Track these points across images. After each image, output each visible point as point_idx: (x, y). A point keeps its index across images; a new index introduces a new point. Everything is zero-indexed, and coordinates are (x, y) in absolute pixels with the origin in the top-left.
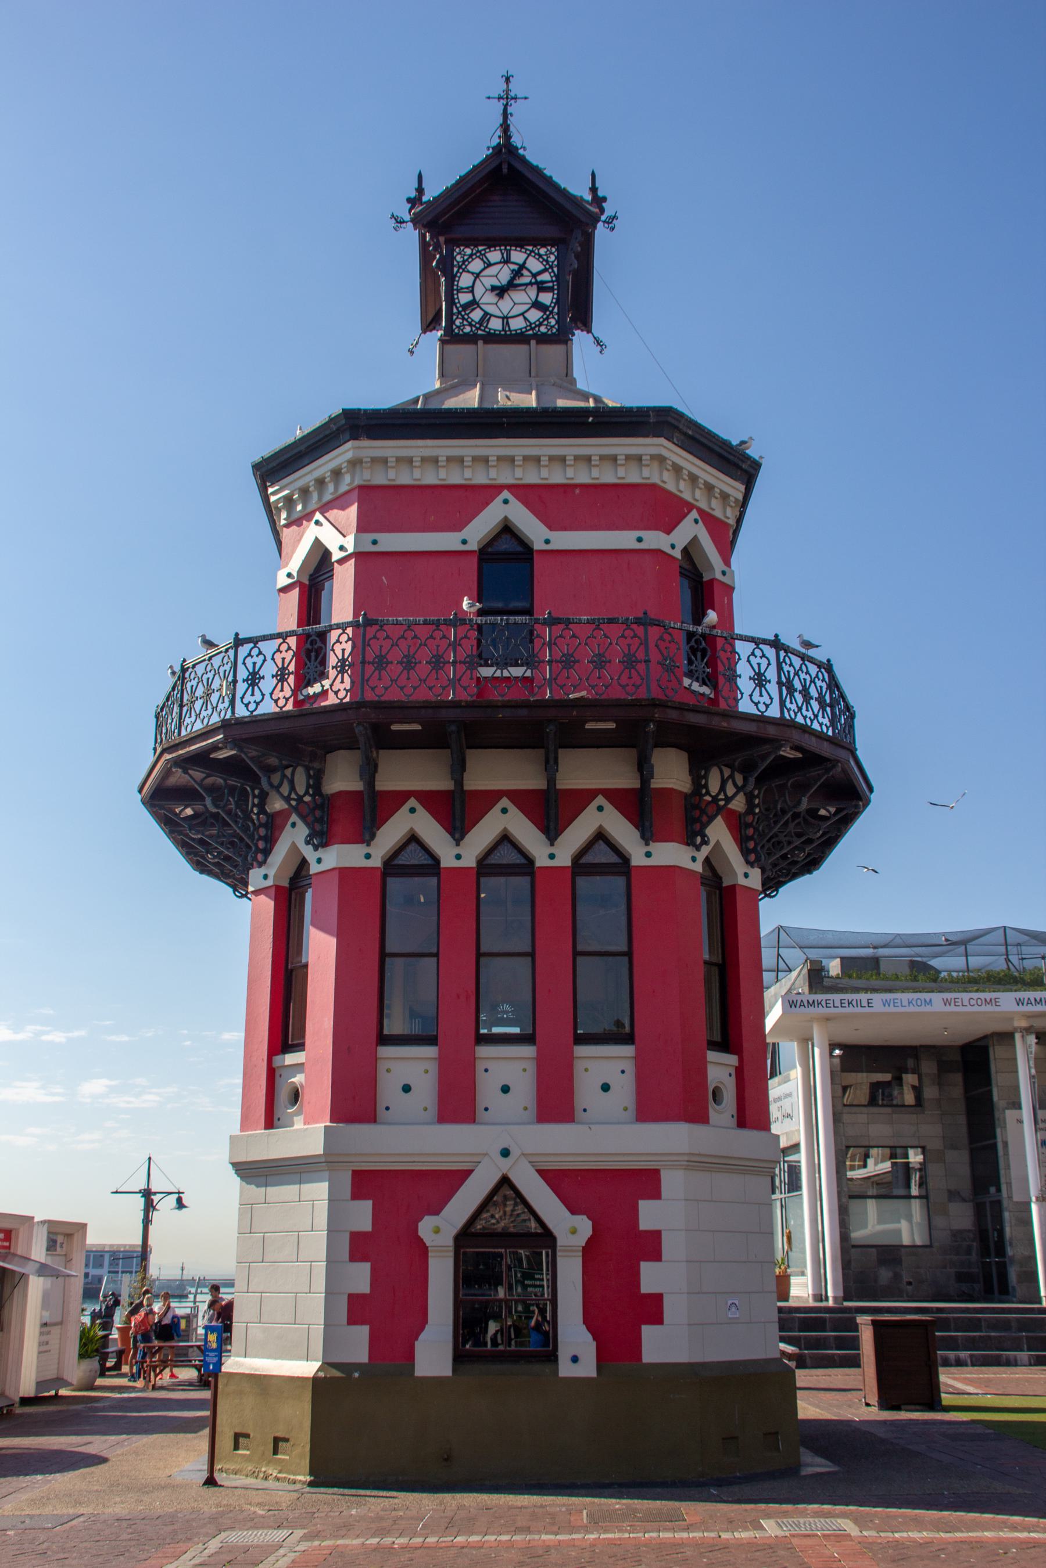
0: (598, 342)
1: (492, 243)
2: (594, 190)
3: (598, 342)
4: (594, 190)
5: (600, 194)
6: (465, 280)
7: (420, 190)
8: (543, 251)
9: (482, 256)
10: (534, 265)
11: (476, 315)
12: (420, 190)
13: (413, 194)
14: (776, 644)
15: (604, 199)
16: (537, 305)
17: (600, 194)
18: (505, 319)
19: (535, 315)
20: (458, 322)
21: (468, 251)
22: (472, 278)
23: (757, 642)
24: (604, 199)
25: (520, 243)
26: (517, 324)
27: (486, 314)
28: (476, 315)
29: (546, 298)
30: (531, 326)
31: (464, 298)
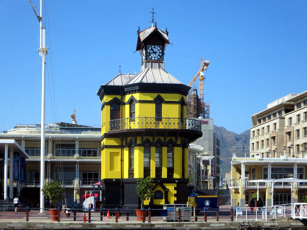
1: (153, 44)
2: (166, 31)
4: (166, 31)
5: (168, 32)
6: (148, 51)
7: (139, 30)
8: (160, 46)
9: (151, 47)
10: (159, 49)
11: (150, 57)
12: (139, 30)
15: (168, 33)
16: (159, 55)
17: (168, 32)
19: (159, 57)
20: (147, 58)
21: (149, 45)
22: (149, 50)
24: (168, 33)
25: (157, 45)
26: (156, 59)
27: (152, 57)
29: (160, 54)
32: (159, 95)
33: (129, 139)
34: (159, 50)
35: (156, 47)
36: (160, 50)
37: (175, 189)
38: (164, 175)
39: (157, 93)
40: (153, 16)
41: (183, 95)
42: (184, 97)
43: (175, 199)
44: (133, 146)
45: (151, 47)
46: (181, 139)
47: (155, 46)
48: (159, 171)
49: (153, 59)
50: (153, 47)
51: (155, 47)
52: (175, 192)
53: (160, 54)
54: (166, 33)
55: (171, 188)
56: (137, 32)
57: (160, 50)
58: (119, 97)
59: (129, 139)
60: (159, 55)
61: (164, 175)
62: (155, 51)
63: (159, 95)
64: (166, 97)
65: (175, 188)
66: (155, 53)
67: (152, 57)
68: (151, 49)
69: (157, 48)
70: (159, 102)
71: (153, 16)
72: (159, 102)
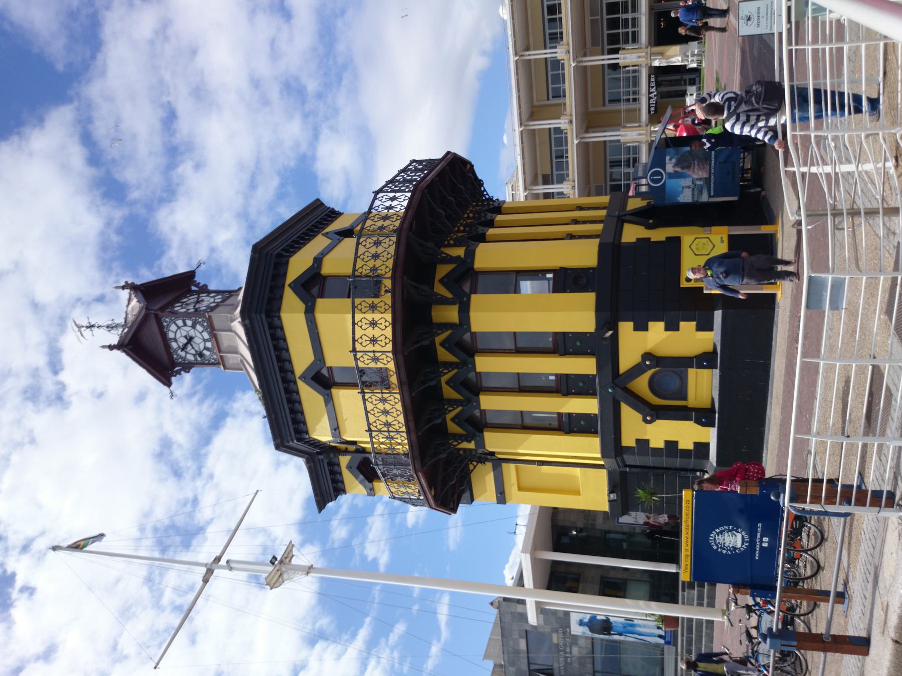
1: (167, 347)
4: (123, 288)
6: (190, 358)
8: (165, 324)
9: (176, 351)
10: (173, 327)
18: (205, 341)
19: (199, 328)
25: (164, 335)
26: (206, 335)
28: (207, 353)
29: (189, 323)
30: (205, 329)
31: (199, 359)
32: (300, 378)
34: (179, 328)
35: (171, 335)
36: (176, 325)
37: (641, 326)
38: (586, 366)
39: (295, 383)
40: (99, 327)
43: (688, 327)
45: (176, 351)
48: (567, 386)
49: (209, 345)
50: (174, 345)
51: (175, 340)
52: (657, 328)
53: (189, 323)
55: (635, 343)
57: (176, 325)
58: (344, 460)
61: (586, 366)
62: (185, 341)
63: (300, 378)
64: (301, 357)
65: (636, 329)
66: (190, 340)
67: (206, 348)
68: (183, 350)
69: (175, 333)
70: (324, 380)
71: (99, 327)
72: (324, 380)
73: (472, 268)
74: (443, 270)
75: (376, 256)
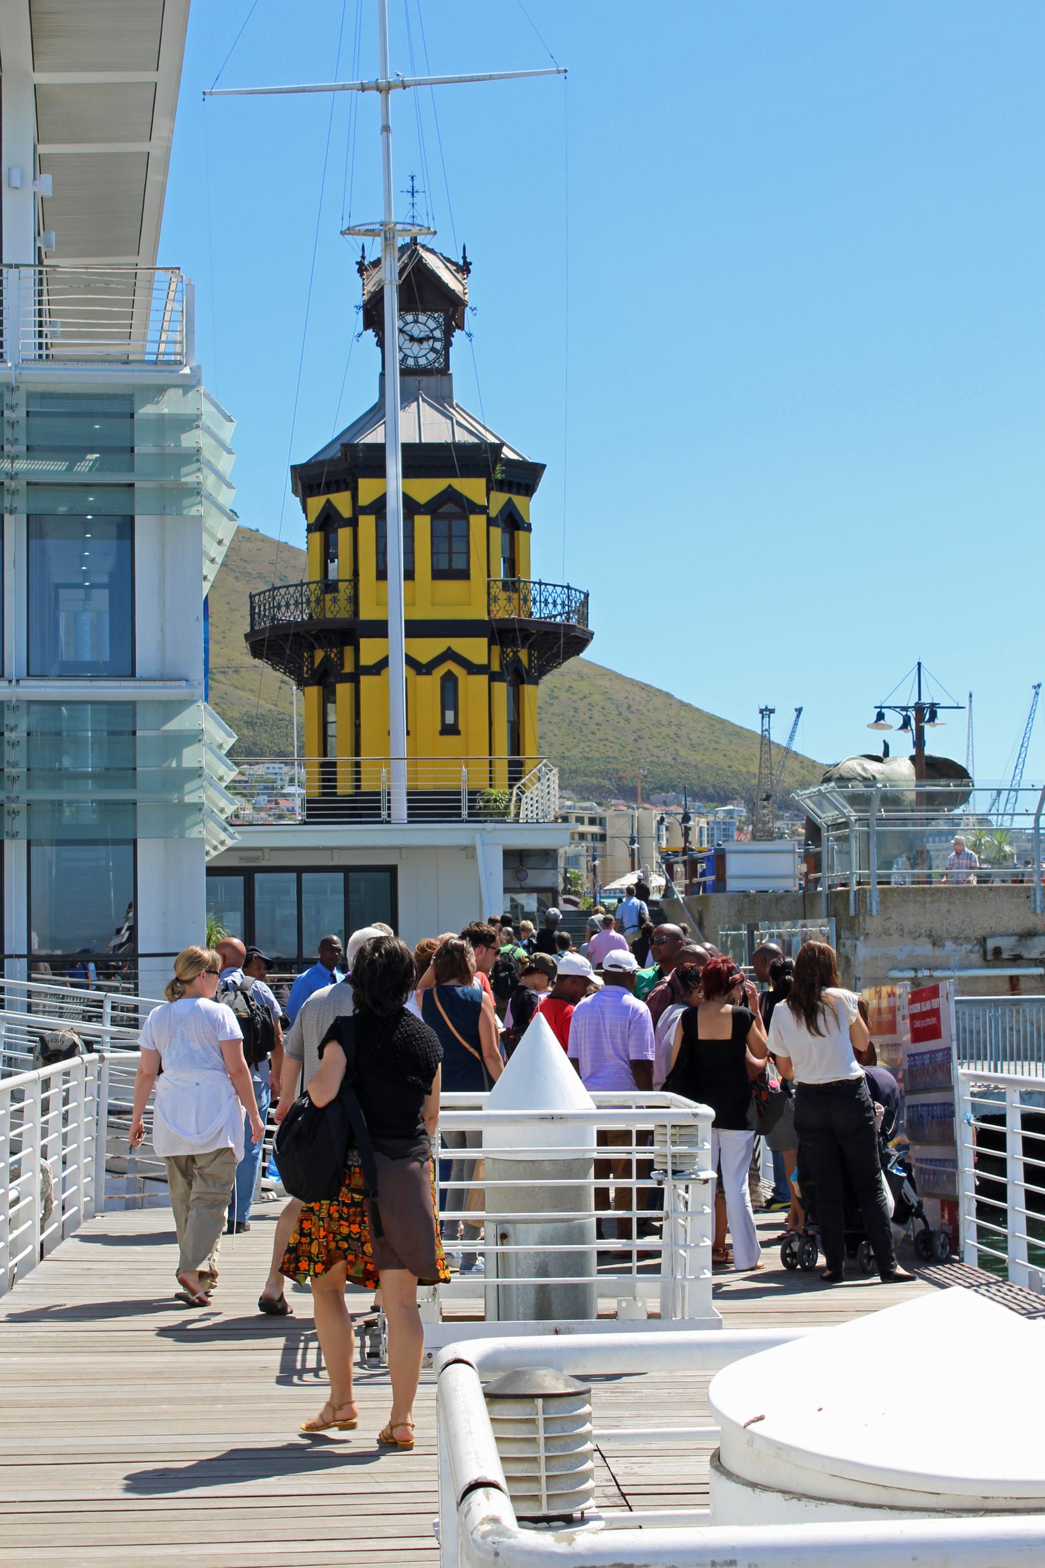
0: (469, 335)
2: (464, 258)
3: (469, 335)
4: (464, 258)
5: (468, 260)
7: (363, 257)
8: (436, 315)
10: (432, 324)
12: (363, 257)
13: (359, 260)
14: (540, 584)
15: (471, 263)
16: (433, 349)
17: (468, 260)
18: (416, 358)
19: (432, 356)
23: (535, 583)
24: (471, 263)
25: (424, 311)
26: (422, 362)
29: (438, 345)
33: (319, 655)
35: (422, 318)
36: (435, 329)
41: (510, 492)
42: (518, 500)
44: (333, 680)
46: (503, 652)
47: (417, 315)
51: (416, 321)
53: (438, 345)
54: (461, 263)
56: (357, 263)
57: (435, 329)
59: (319, 655)
60: (433, 349)
73: (523, 682)
74: (523, 655)
75: (555, 604)
